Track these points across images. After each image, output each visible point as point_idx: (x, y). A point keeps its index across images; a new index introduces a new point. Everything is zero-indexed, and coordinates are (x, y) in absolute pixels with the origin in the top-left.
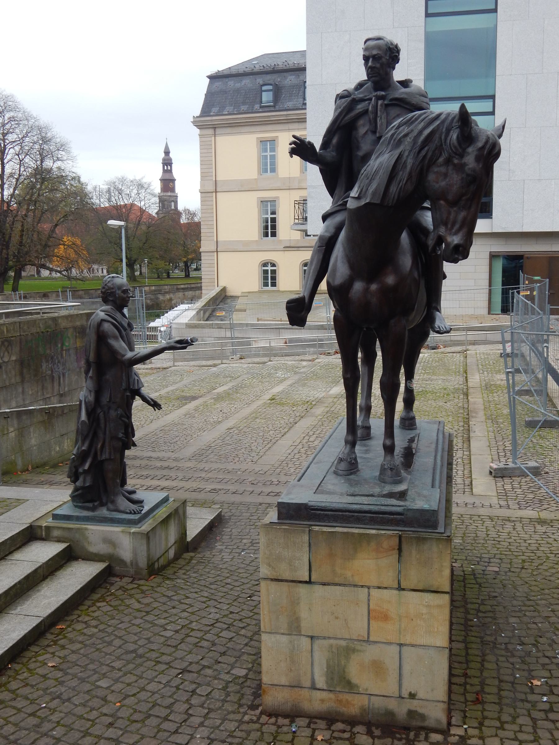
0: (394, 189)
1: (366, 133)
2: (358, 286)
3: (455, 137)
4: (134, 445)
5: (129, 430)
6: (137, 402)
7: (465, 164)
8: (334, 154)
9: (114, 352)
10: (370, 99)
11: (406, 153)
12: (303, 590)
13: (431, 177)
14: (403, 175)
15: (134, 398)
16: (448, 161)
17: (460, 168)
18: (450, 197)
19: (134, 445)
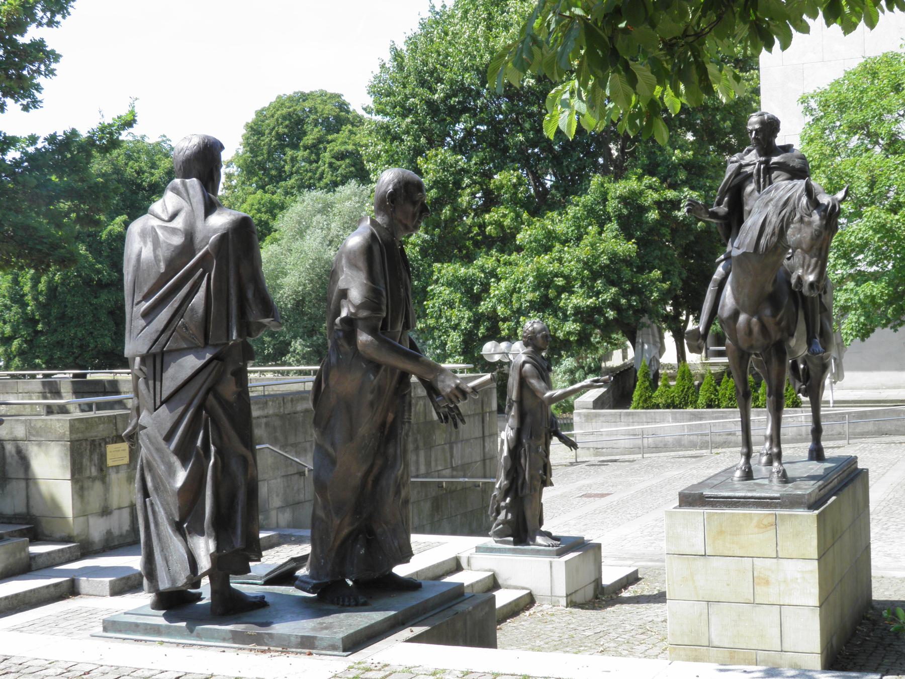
0: (763, 241)
1: (753, 191)
2: (742, 318)
3: (805, 202)
4: (551, 484)
5: (546, 469)
6: (555, 440)
7: (813, 222)
8: (726, 209)
9: (533, 392)
10: (755, 164)
11: (771, 213)
12: (701, 562)
13: (790, 231)
14: (769, 230)
15: (551, 438)
16: (801, 220)
17: (810, 224)
18: (804, 246)
19: (551, 484)
